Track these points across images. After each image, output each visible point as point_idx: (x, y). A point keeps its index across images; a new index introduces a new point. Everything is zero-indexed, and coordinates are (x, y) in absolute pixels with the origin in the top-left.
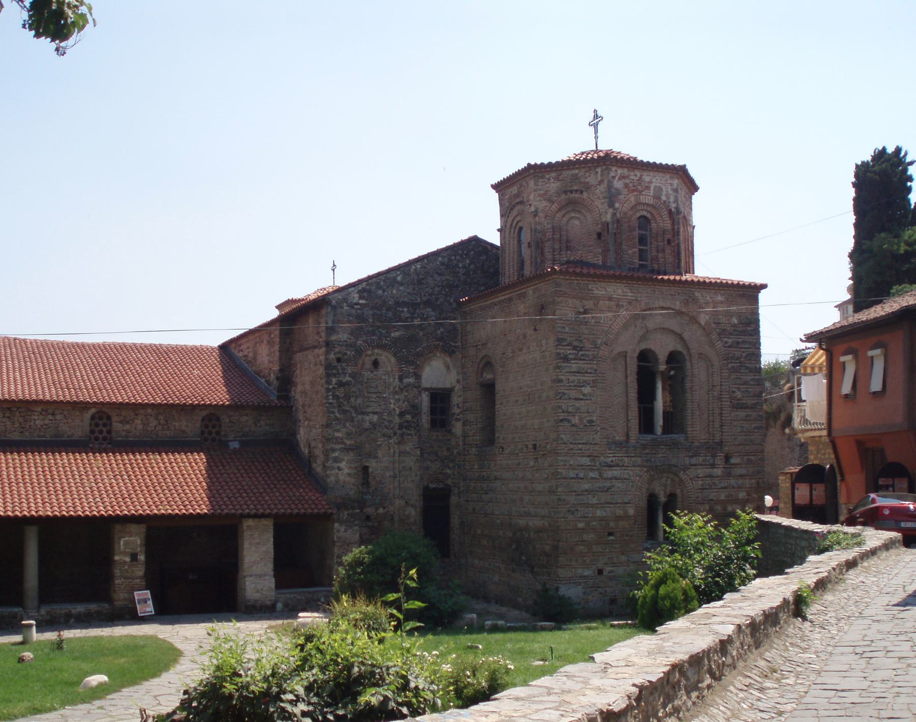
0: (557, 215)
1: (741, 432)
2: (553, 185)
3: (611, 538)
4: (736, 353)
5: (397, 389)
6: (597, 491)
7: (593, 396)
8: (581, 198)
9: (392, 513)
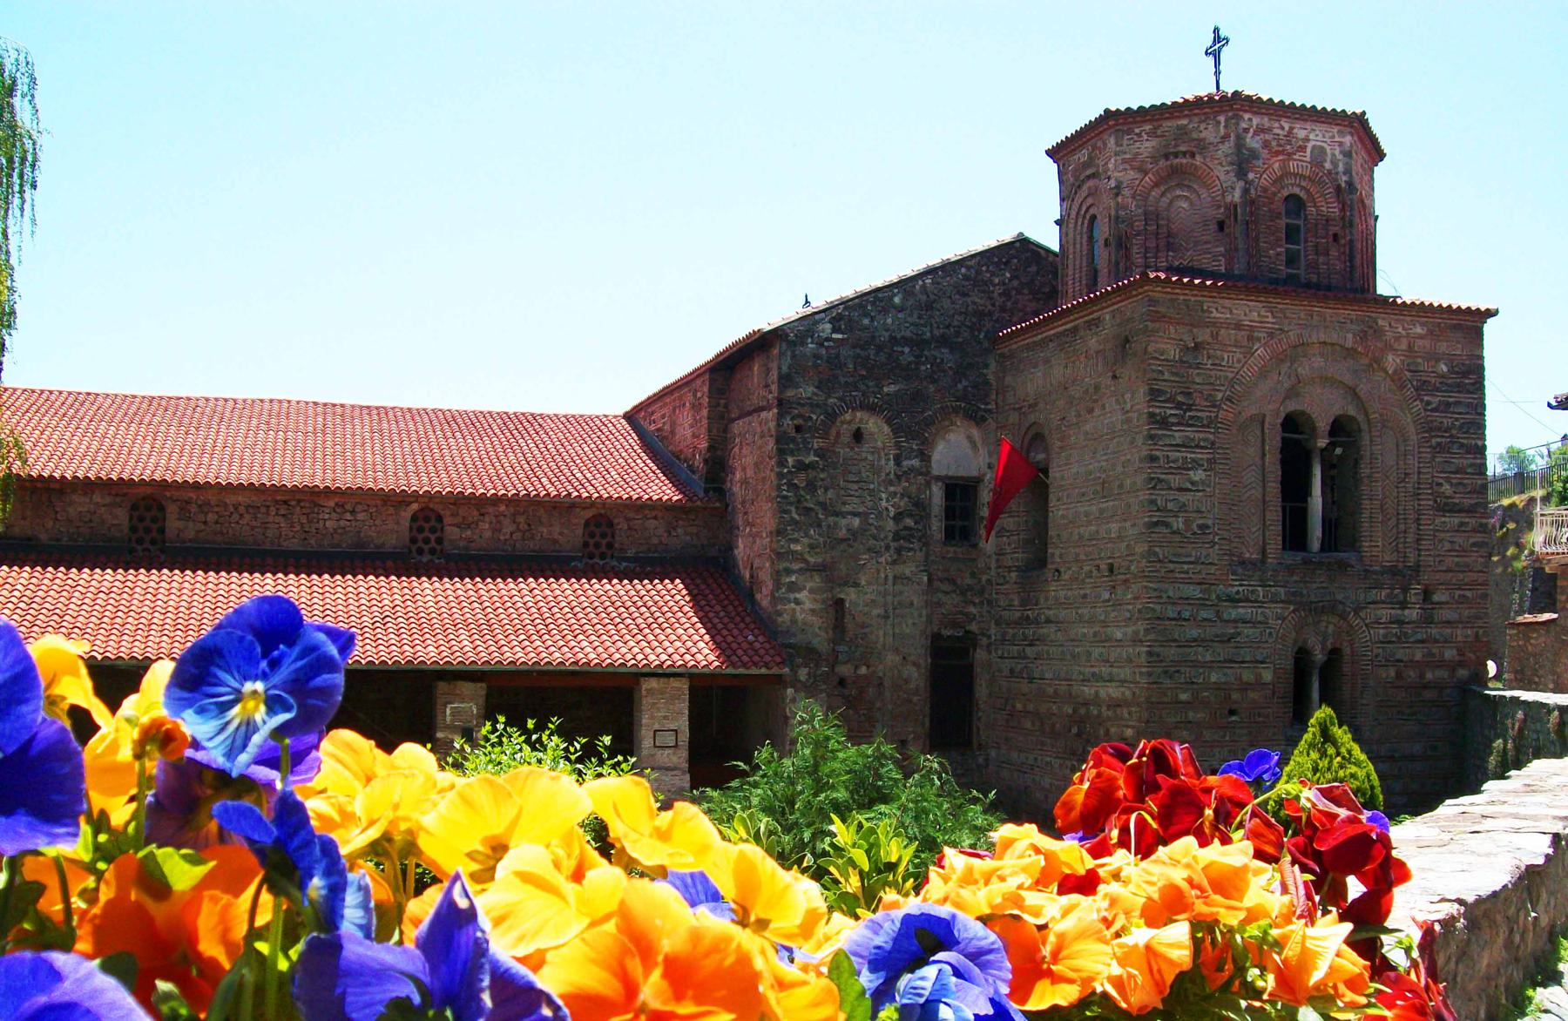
1: (1450, 551)
2: (1148, 144)
3: (1234, 718)
4: (1445, 421)
5: (892, 476)
6: (1212, 641)
7: (1209, 486)
8: (1192, 164)
9: (881, 674)
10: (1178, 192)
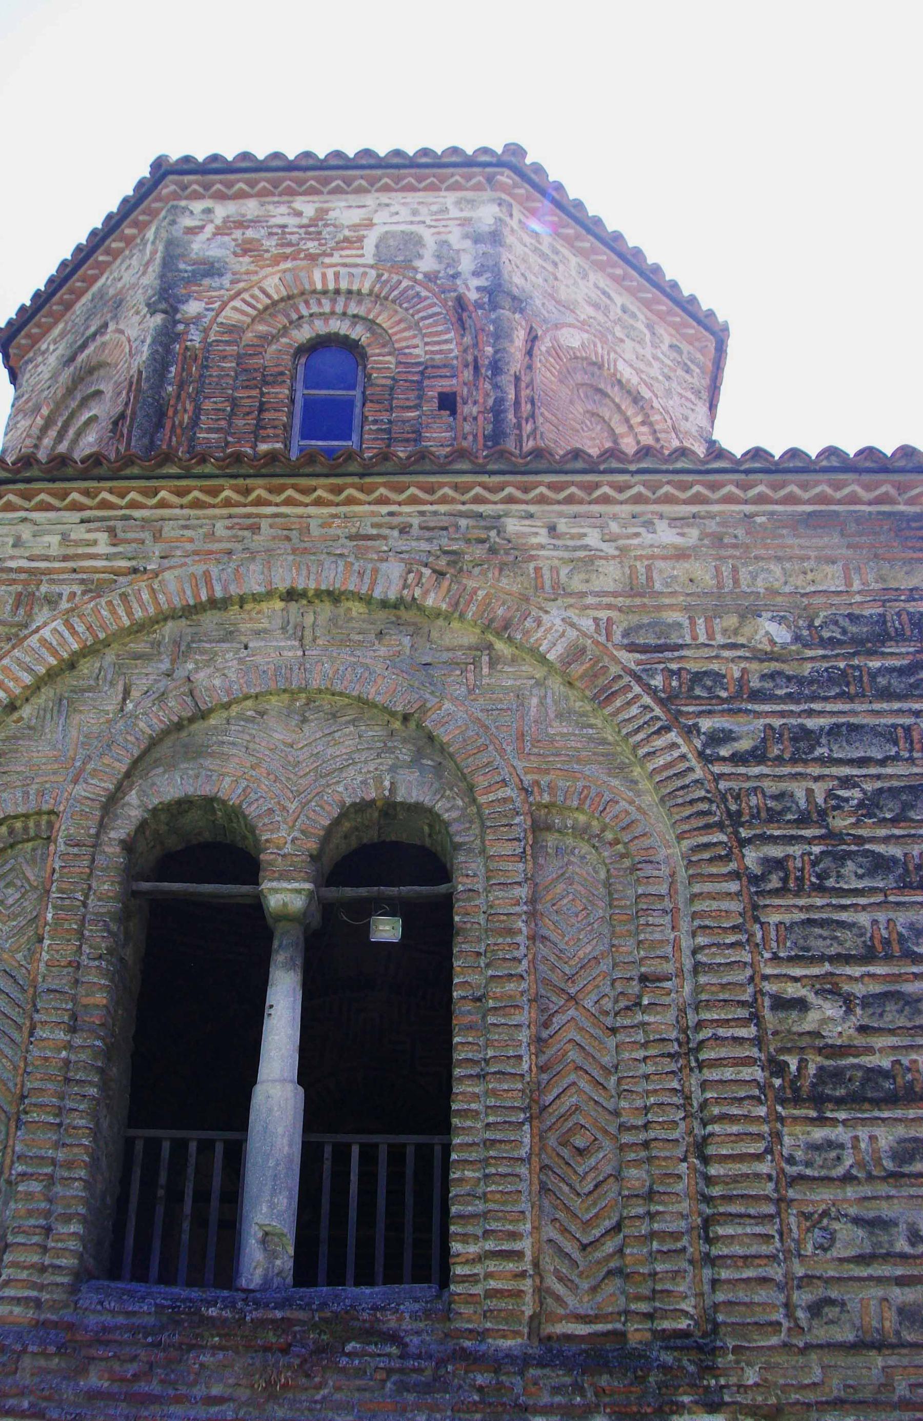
1: (862, 1259)
4: (799, 790)
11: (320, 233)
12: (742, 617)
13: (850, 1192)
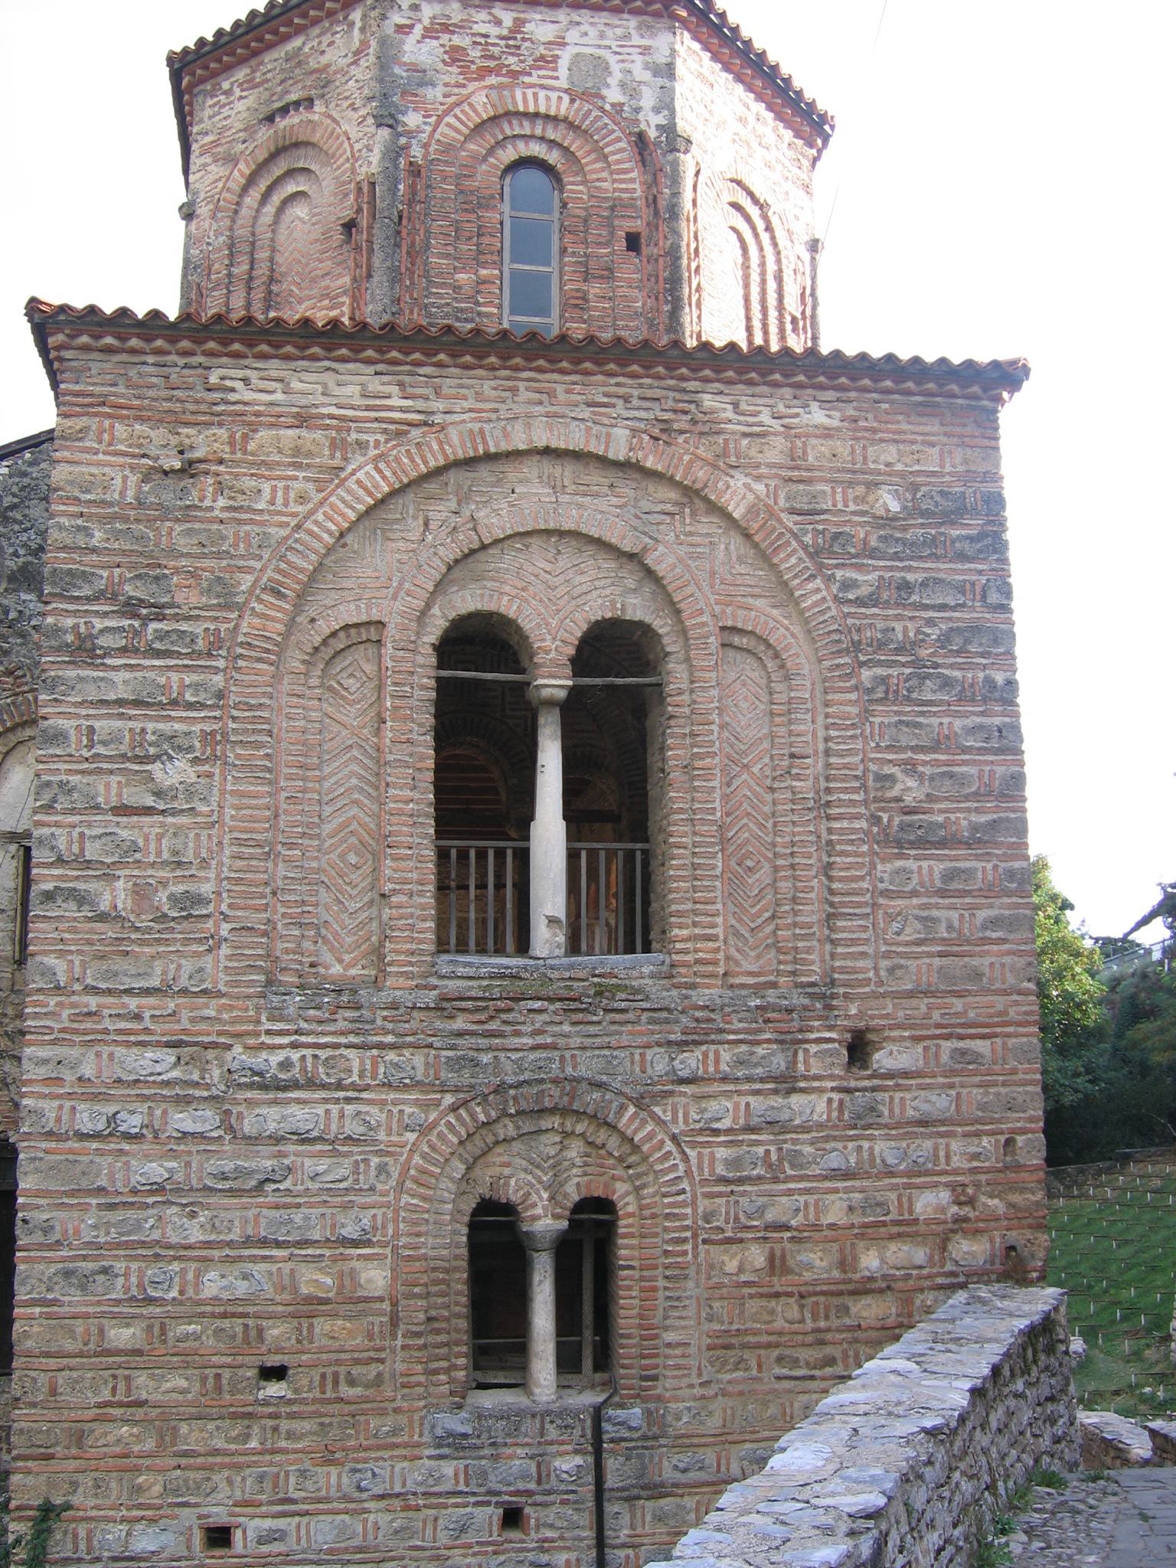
0: (248, 200)
1: (919, 943)
2: (240, 106)
3: (275, 1389)
4: (899, 627)
6: (211, 1189)
10: (291, 188)
11: (518, 47)
12: (868, 488)
13: (915, 901)
